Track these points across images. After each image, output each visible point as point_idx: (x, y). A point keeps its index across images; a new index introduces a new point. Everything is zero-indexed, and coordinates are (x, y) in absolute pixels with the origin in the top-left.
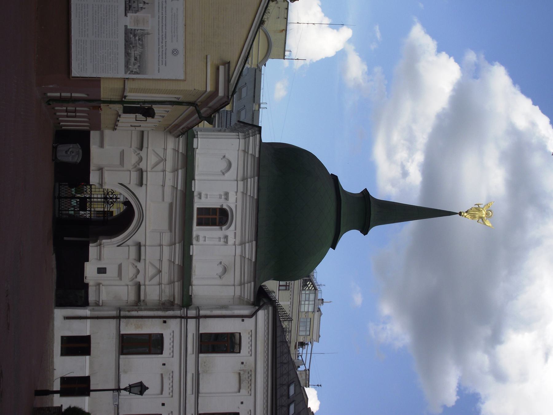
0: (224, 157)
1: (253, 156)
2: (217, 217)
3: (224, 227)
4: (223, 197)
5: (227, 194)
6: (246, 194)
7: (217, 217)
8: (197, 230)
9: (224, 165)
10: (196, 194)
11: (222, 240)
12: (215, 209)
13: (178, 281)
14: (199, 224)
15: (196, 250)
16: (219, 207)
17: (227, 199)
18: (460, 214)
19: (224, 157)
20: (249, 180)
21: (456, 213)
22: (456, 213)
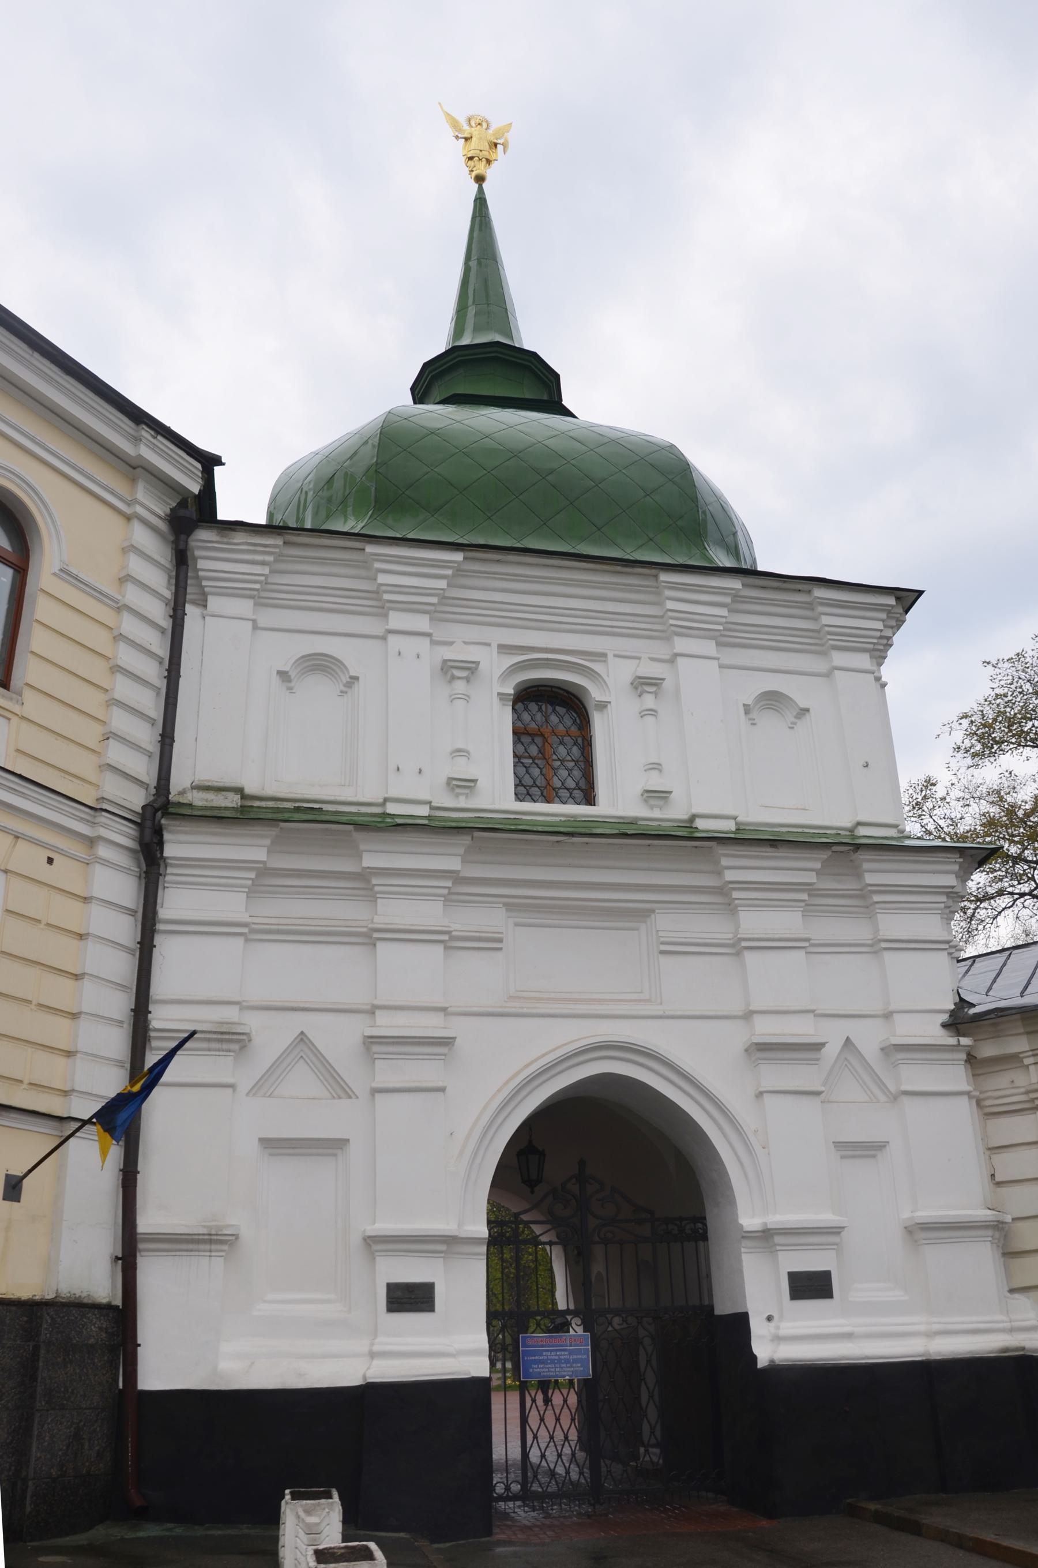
0: (283, 675)
1: (279, 558)
2: (552, 719)
3: (595, 693)
4: (460, 686)
5: (449, 670)
6: (443, 598)
7: (552, 719)
8: (618, 797)
9: (318, 689)
10: (447, 801)
11: (649, 701)
12: (519, 734)
13: (859, 876)
14: (589, 798)
15: (714, 794)
16: (509, 710)
17: (471, 669)
18: (480, 179)
19: (283, 675)
20: (382, 579)
21: (481, 190)
22: (481, 190)
